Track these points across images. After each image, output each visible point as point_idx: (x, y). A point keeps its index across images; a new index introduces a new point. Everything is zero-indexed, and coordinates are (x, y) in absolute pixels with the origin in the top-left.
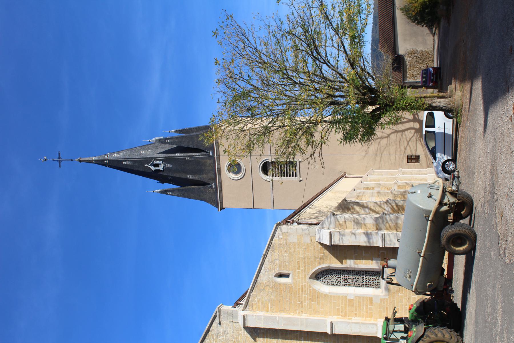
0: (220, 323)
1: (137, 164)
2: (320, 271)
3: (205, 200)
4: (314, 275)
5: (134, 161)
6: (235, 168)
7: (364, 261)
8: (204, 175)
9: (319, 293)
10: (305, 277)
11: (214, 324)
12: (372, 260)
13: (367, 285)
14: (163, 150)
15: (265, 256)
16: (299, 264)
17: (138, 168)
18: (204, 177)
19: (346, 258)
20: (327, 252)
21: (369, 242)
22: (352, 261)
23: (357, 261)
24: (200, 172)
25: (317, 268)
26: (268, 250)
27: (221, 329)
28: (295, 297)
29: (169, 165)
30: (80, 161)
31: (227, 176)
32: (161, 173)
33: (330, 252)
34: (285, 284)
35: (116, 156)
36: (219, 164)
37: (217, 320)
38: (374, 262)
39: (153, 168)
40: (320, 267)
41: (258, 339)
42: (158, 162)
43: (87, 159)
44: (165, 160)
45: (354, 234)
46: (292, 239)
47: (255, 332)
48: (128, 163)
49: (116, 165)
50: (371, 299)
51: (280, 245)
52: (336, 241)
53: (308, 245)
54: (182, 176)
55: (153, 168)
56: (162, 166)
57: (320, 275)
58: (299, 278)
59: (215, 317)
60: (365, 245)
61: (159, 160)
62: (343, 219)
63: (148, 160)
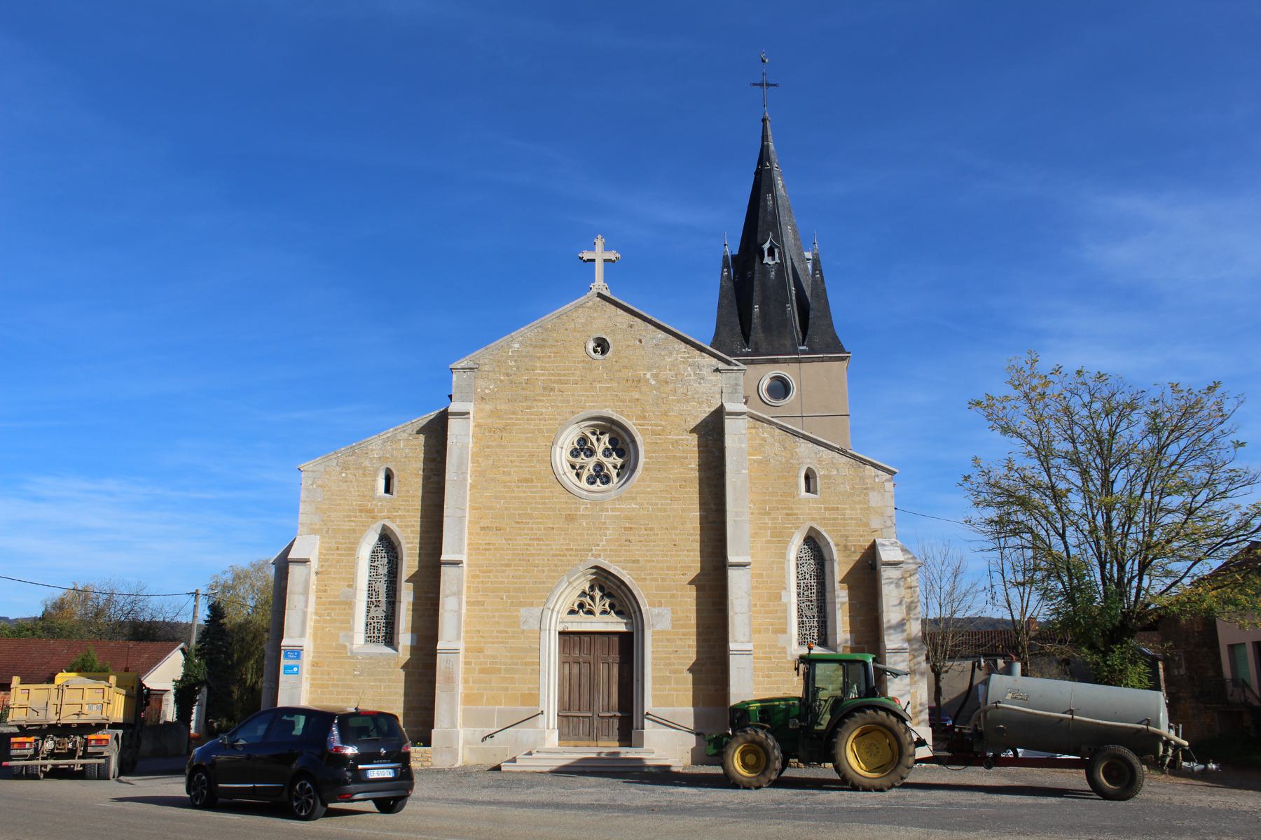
0: (717, 370)
1: (769, 218)
2: (821, 544)
3: (717, 334)
4: (813, 535)
5: (775, 214)
6: (781, 388)
7: (847, 619)
8: (761, 335)
9: (787, 543)
10: (813, 519)
11: (714, 361)
12: (851, 632)
13: (801, 624)
14: (796, 265)
15: (843, 452)
16: (833, 509)
17: (759, 219)
18: (757, 334)
19: (849, 588)
20: (857, 557)
21: (890, 628)
22: (847, 599)
23: (847, 607)
24: (767, 329)
25: (829, 540)
26: (854, 457)
27: (706, 372)
28: (777, 502)
29: (773, 275)
30: (764, 120)
31: (766, 374)
32: (757, 259)
33: (858, 562)
34: (797, 484)
35: (779, 182)
36: (785, 361)
37: (721, 366)
38: (848, 636)
39: (766, 246)
40: (832, 544)
41: (695, 436)
42: (777, 255)
43: (770, 133)
44: (781, 267)
45: (900, 603)
46: (874, 499)
47: (711, 433)
48: (770, 203)
49: (762, 183)
50: (784, 631)
51: (862, 478)
52: (887, 574)
53: (867, 525)
54: (757, 295)
55: (766, 246)
56: (771, 263)
57: (814, 542)
58: (810, 511)
59: (729, 363)
60: (885, 620)
61: (780, 258)
62: (914, 584)
63: (778, 237)
